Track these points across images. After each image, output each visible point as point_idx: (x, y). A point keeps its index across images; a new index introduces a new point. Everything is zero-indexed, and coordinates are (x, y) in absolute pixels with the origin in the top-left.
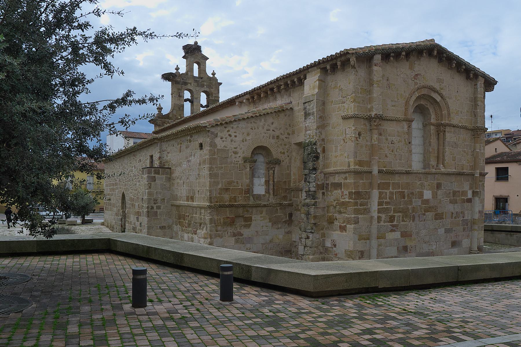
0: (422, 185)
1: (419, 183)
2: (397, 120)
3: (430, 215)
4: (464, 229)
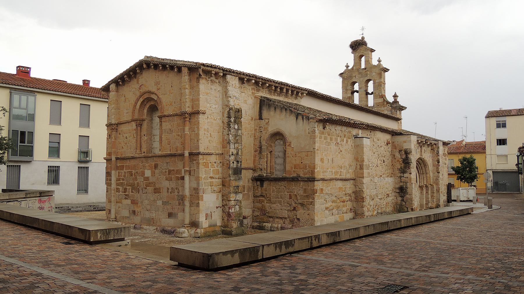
0: (144, 166)
1: (141, 165)
2: (128, 122)
3: (150, 189)
4: (179, 204)
